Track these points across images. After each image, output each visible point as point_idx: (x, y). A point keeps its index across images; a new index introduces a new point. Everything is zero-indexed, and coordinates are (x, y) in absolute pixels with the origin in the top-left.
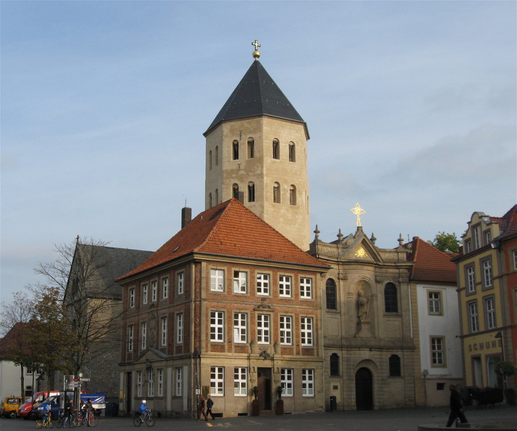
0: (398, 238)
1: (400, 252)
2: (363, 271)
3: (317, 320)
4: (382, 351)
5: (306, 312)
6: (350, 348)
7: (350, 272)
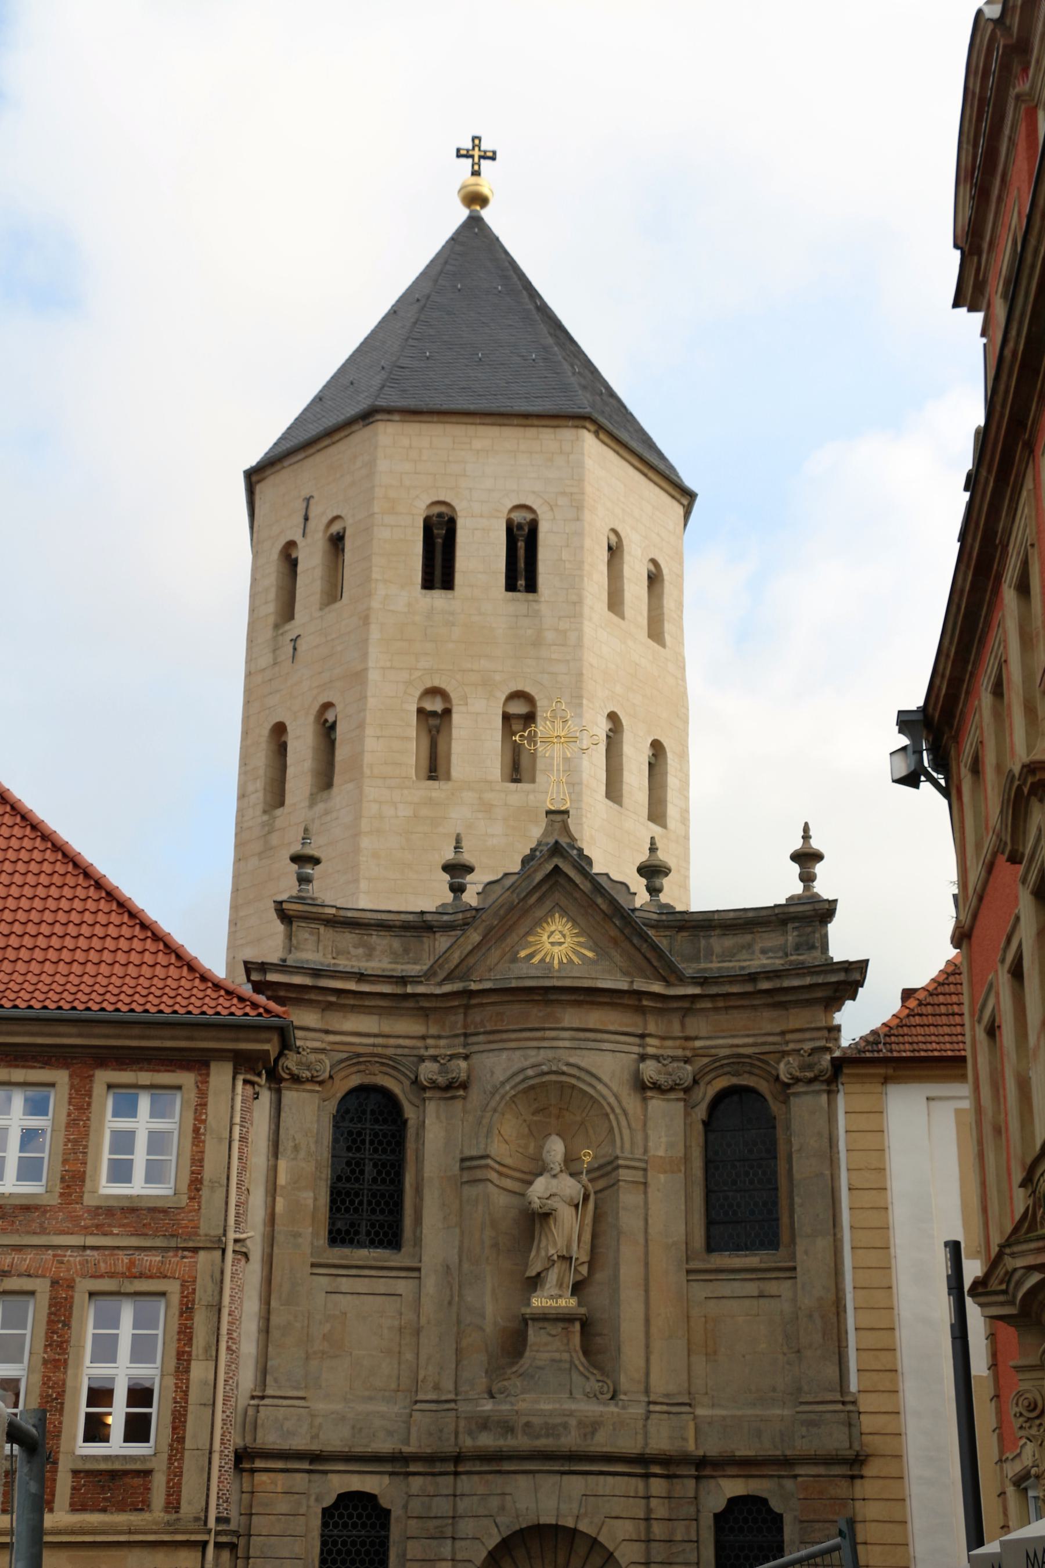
3: (187, 1310)
5: (120, 1268)
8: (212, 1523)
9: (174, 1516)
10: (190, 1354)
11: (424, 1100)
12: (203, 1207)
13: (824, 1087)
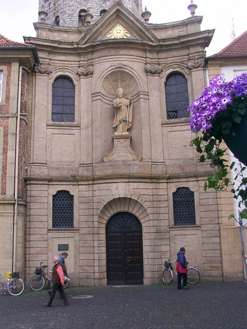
0: (190, 4)
1: (189, 23)
2: (117, 56)
4: (159, 183)
6: (93, 180)
7: (97, 62)
8: (16, 198)
9: (4, 196)
10: (7, 148)
11: (80, 79)
12: (10, 105)
13: (203, 69)
